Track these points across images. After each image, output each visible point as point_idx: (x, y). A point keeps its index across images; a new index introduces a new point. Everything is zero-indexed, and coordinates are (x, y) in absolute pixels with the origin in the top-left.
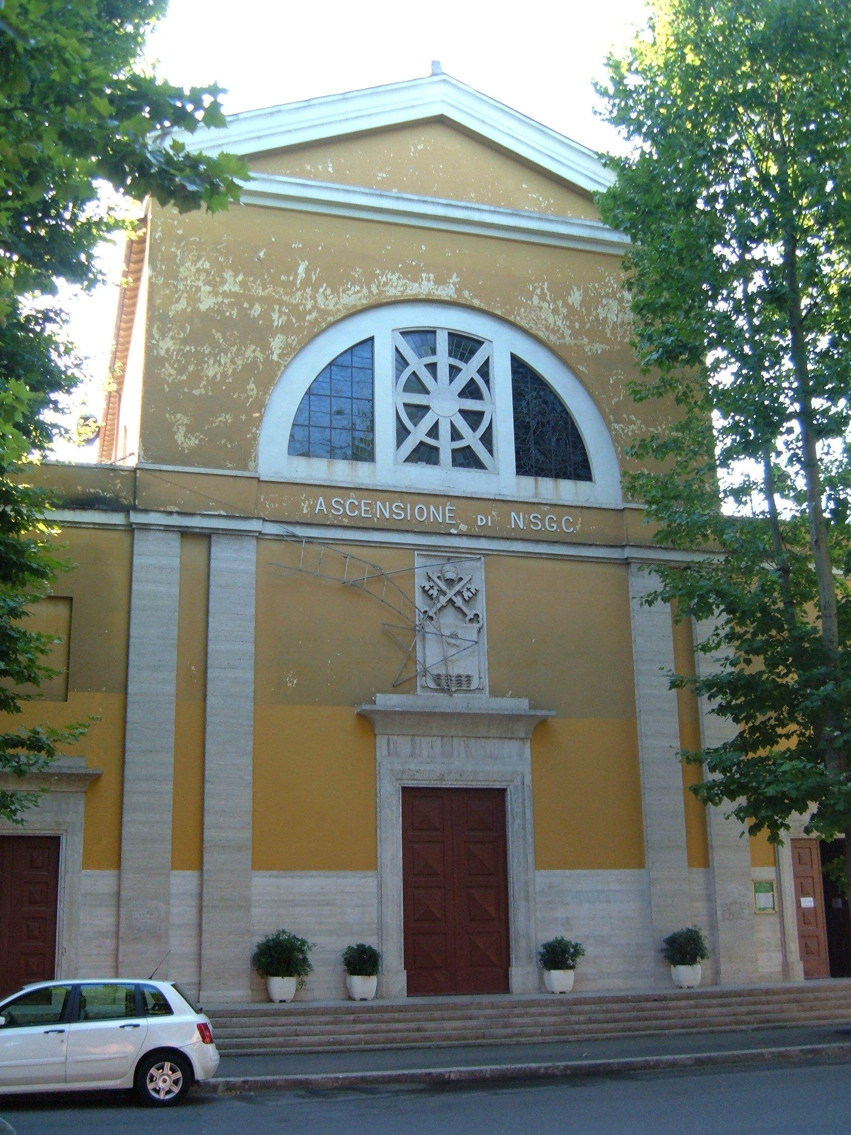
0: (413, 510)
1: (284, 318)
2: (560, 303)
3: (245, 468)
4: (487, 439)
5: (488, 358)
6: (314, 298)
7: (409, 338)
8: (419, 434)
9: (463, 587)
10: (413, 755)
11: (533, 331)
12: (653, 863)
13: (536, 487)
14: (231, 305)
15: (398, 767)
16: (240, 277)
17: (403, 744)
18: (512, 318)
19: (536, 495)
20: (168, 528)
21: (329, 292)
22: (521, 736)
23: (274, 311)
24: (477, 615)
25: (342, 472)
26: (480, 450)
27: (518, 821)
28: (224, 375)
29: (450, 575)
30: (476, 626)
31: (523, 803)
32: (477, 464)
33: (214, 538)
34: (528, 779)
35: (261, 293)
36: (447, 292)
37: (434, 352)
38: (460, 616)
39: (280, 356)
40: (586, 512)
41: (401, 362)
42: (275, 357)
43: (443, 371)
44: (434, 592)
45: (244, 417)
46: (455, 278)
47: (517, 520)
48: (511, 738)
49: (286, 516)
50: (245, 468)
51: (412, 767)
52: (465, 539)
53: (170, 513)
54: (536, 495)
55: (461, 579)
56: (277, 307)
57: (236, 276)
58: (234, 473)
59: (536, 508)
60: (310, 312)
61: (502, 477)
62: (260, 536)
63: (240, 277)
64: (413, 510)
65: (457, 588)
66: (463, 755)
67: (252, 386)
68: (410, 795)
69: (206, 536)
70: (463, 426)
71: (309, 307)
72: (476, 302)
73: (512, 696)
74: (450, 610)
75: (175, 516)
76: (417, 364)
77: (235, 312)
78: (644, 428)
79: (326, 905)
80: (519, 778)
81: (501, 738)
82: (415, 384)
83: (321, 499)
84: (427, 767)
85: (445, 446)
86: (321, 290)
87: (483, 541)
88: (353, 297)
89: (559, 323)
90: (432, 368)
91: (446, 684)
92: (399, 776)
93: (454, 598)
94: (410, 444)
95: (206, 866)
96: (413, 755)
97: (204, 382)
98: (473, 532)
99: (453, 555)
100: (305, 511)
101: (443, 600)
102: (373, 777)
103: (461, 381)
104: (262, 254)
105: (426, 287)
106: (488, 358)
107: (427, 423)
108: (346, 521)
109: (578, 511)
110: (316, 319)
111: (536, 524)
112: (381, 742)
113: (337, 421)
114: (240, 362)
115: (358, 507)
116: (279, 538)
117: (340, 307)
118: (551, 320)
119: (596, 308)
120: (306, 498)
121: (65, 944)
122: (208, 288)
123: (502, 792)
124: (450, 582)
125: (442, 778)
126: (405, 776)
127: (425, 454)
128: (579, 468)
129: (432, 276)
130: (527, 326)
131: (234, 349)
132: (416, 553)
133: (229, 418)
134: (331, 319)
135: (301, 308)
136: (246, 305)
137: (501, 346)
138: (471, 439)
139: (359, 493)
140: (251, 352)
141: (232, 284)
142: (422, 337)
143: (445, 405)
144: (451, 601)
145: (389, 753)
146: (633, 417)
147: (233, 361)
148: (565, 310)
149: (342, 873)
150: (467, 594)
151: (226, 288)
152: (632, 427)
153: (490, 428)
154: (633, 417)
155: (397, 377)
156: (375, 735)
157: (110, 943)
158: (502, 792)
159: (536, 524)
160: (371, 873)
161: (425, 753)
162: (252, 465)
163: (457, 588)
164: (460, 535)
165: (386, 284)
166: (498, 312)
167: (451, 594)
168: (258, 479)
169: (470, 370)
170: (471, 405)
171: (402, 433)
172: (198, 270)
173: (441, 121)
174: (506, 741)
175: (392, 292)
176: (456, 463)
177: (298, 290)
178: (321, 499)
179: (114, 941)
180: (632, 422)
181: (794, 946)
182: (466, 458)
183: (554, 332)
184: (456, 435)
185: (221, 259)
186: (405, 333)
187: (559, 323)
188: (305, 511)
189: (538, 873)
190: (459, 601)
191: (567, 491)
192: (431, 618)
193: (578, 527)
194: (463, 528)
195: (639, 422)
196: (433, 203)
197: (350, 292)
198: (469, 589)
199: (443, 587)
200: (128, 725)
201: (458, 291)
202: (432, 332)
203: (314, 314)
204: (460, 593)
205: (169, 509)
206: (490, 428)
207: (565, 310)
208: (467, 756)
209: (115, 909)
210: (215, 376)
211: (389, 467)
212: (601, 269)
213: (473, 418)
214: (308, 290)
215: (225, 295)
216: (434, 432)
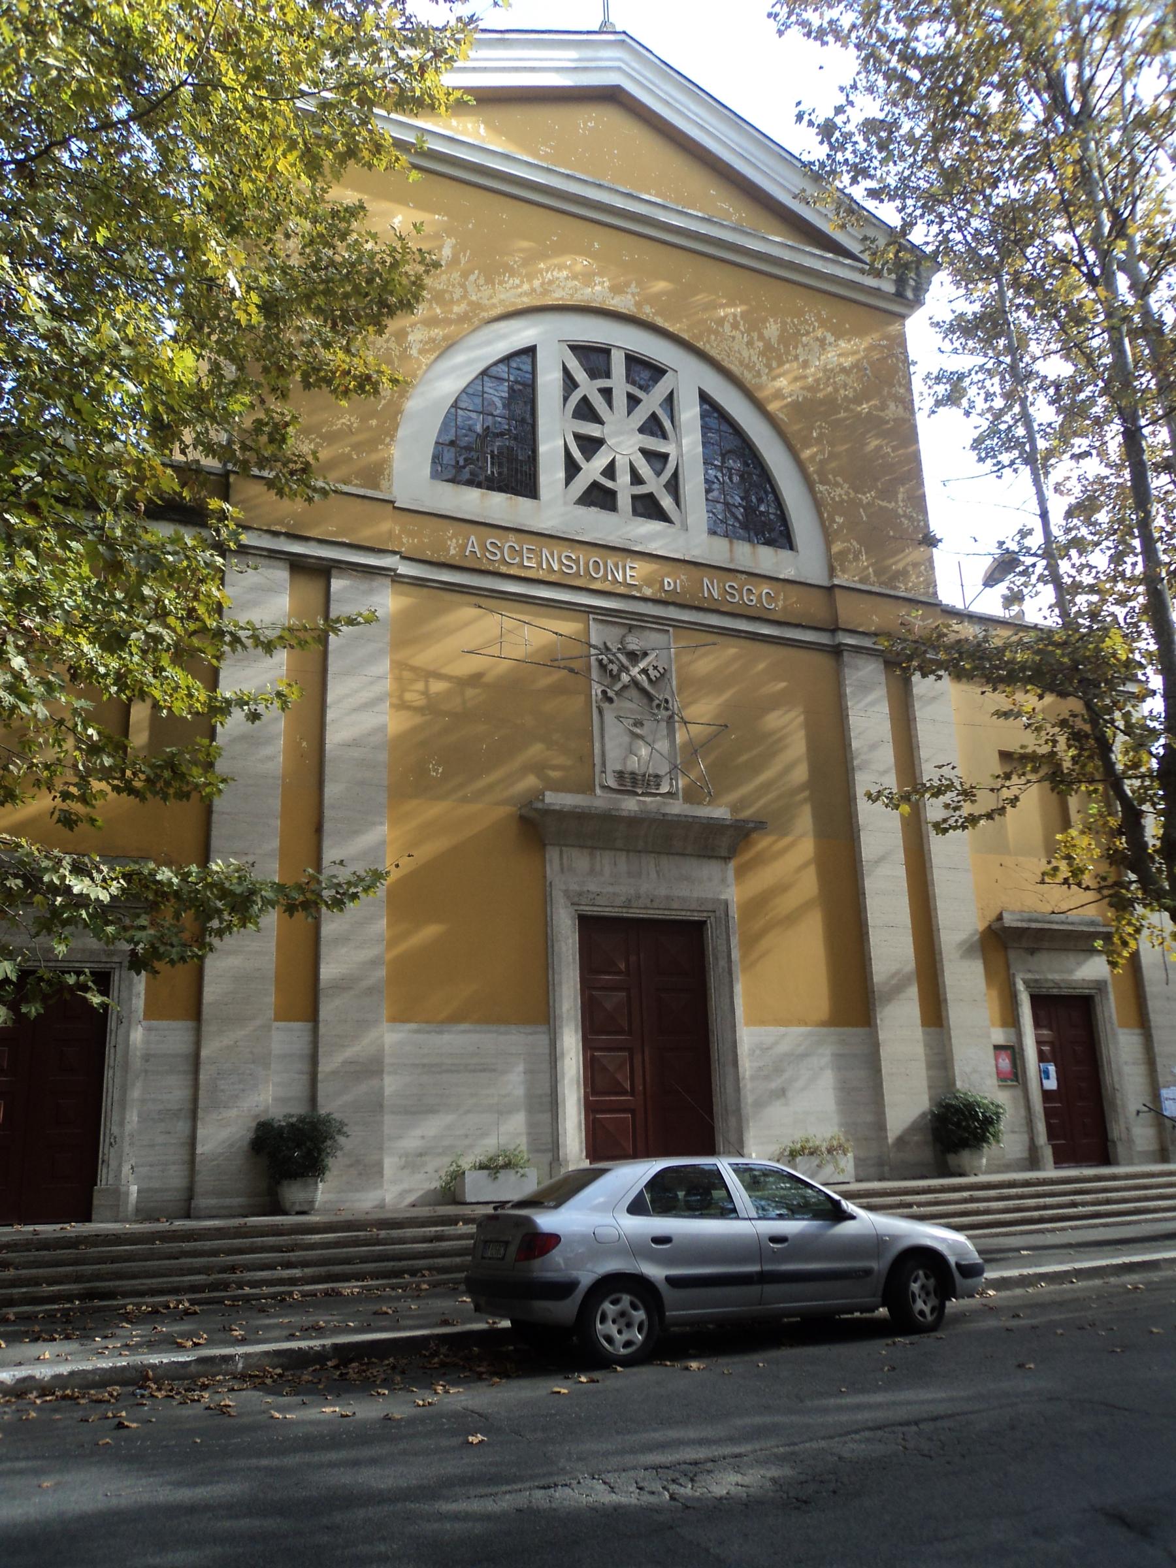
0: (587, 564)
2: (755, 335)
3: (376, 486)
4: (673, 486)
5: (672, 393)
6: (463, 286)
8: (592, 470)
10: (592, 871)
11: (725, 364)
13: (731, 551)
15: (574, 887)
17: (580, 860)
18: (700, 345)
19: (732, 560)
20: (273, 555)
21: (482, 281)
25: (497, 506)
26: (666, 502)
27: (723, 963)
29: (631, 647)
32: (661, 515)
33: (334, 572)
36: (623, 303)
37: (608, 375)
38: (645, 701)
40: (789, 587)
41: (570, 383)
42: (414, 352)
43: (620, 400)
44: (614, 668)
47: (712, 588)
48: (710, 857)
49: (428, 555)
50: (376, 486)
51: (592, 887)
52: (650, 604)
53: (276, 534)
54: (732, 560)
55: (645, 654)
58: (361, 492)
59: (731, 575)
60: (458, 302)
61: (691, 534)
62: (397, 579)
64: (587, 564)
65: (642, 665)
66: (653, 875)
68: (589, 925)
69: (322, 571)
70: (644, 469)
71: (456, 296)
72: (660, 322)
74: (633, 693)
75: (282, 538)
76: (588, 387)
78: (852, 494)
79: (484, 1070)
80: (722, 907)
81: (699, 856)
82: (586, 411)
83: (473, 538)
84: (610, 889)
86: (472, 278)
87: (671, 609)
89: (754, 358)
90: (607, 393)
91: (631, 782)
92: (576, 900)
94: (581, 483)
95: (323, 1014)
98: (658, 596)
99: (634, 623)
100: (452, 552)
102: (546, 900)
103: (641, 415)
105: (598, 292)
106: (672, 393)
107: (600, 461)
109: (780, 585)
110: (466, 313)
111: (733, 596)
112: (553, 854)
116: (419, 583)
118: (745, 354)
119: (796, 348)
120: (454, 536)
121: (115, 1130)
123: (700, 926)
124: (634, 657)
125: (628, 905)
127: (600, 497)
128: (777, 533)
130: (718, 358)
135: (447, 296)
137: (688, 379)
138: (654, 484)
142: (595, 358)
144: (634, 682)
145: (562, 870)
146: (839, 479)
148: (761, 344)
149: (503, 1028)
152: (839, 491)
153: (675, 475)
154: (839, 479)
155: (566, 399)
156: (544, 845)
157: (182, 1127)
158: (700, 926)
159: (733, 596)
160: (544, 1028)
161: (607, 870)
162: (384, 484)
163: (642, 665)
166: (686, 336)
167: (634, 671)
168: (393, 502)
169: (652, 402)
171: (572, 469)
173: (612, 96)
176: (636, 513)
178: (473, 538)
179: (189, 1124)
180: (837, 485)
181: (1041, 1127)
182: (647, 507)
183: (747, 366)
184: (637, 479)
186: (571, 347)
187: (754, 358)
188: (452, 552)
191: (767, 559)
192: (610, 700)
193: (780, 603)
194: (648, 592)
195: (846, 486)
196: (611, 189)
200: (215, 817)
201: (638, 305)
202: (605, 352)
204: (644, 671)
205: (273, 528)
206: (675, 475)
207: (761, 344)
209: (190, 1077)
211: (554, 506)
212: (800, 303)
213: (657, 459)
216: (610, 471)
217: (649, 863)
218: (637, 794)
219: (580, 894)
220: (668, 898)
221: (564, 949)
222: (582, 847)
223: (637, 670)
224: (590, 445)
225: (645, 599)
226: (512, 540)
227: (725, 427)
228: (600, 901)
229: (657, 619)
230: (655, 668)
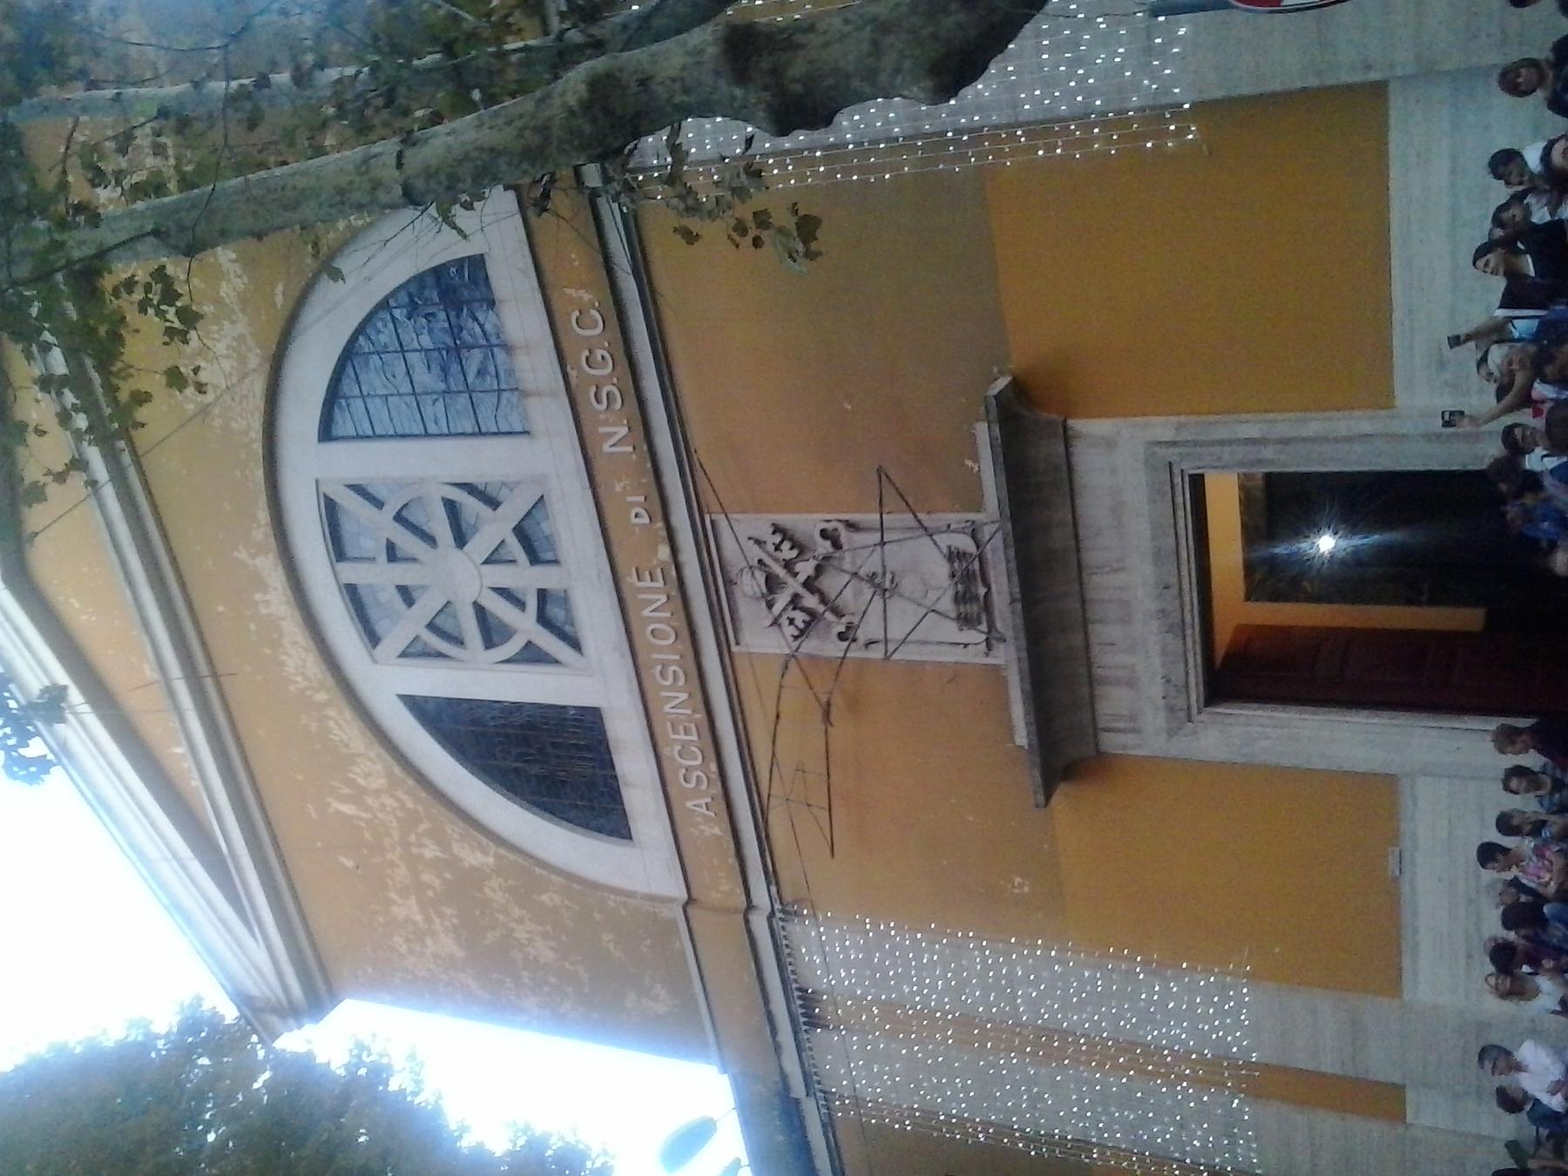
0: (661, 650)
1: (425, 841)
6: (377, 793)
7: (380, 628)
8: (525, 625)
9: (776, 560)
10: (1131, 683)
12: (1369, 67)
14: (441, 916)
16: (394, 896)
21: (355, 769)
22: (1061, 449)
23: (422, 856)
24: (824, 534)
26: (513, 510)
27: (1268, 453)
28: (545, 936)
30: (844, 535)
31: (1222, 443)
34: (1162, 428)
35: (402, 871)
39: (486, 853)
44: (800, 617)
45: (597, 916)
46: (242, 555)
51: (1157, 690)
56: (415, 850)
57: (393, 902)
63: (394, 896)
66: (1119, 579)
67: (545, 898)
73: (976, 459)
77: (449, 911)
83: (689, 804)
84: (1157, 661)
85: (526, 578)
86: (361, 781)
88: (346, 730)
92: (1182, 715)
93: (802, 578)
94: (548, 642)
96: (1131, 683)
97: (567, 965)
100: (717, 831)
101: (811, 601)
104: (349, 863)
107: (500, 609)
108: (714, 767)
113: (552, 761)
114: (517, 912)
115: (685, 745)
117: (372, 754)
122: (429, 941)
124: (772, 584)
126: (1180, 702)
129: (258, 597)
131: (501, 917)
132: (734, 649)
133: (606, 937)
134: (397, 770)
136: (430, 893)
139: (661, 743)
140: (494, 890)
141: (408, 909)
143: (460, 577)
144: (809, 584)
145: (1135, 731)
147: (520, 921)
150: (787, 553)
151: (419, 918)
164: (674, 551)
165: (306, 678)
170: (440, 526)
171: (532, 655)
172: (411, 952)
174: (1076, 478)
175: (313, 666)
177: (375, 816)
178: (689, 804)
185: (381, 920)
189: (1401, 399)
190: (806, 569)
194: (664, 552)
197: (345, 738)
198: (777, 548)
199: (782, 600)
203: (400, 794)
204: (788, 565)
208: (1119, 569)
210: (552, 949)
214: (369, 800)
215: (429, 920)
217: (1102, 586)
218: (987, 595)
219: (1171, 709)
220: (1158, 556)
221: (1266, 744)
222: (1092, 697)
223: (790, 580)
224: (492, 632)
225: (674, 551)
226: (670, 752)
227: (349, 386)
228: (1178, 675)
229: (701, 544)
230: (777, 548)
